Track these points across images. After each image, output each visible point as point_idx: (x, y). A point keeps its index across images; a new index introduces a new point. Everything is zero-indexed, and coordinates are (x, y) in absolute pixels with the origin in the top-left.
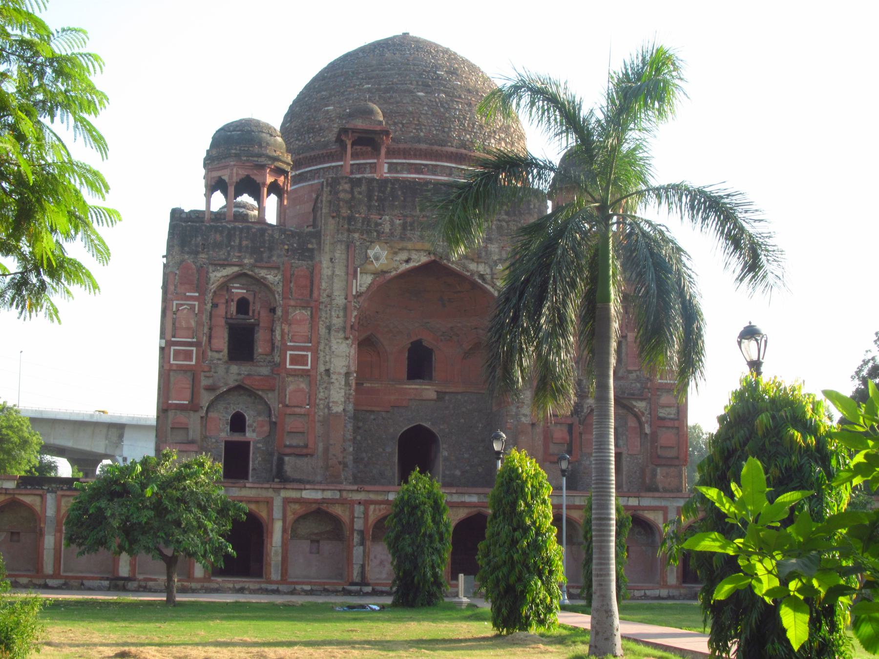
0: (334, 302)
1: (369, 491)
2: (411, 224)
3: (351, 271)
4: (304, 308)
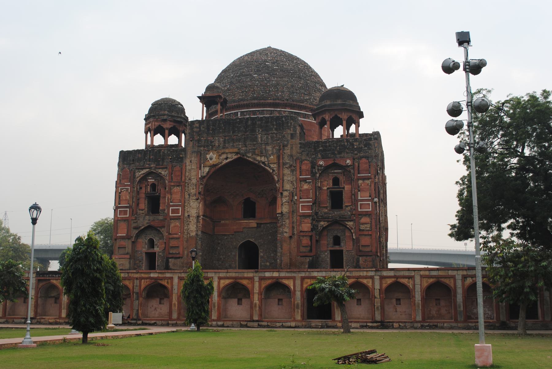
4: (178, 186)
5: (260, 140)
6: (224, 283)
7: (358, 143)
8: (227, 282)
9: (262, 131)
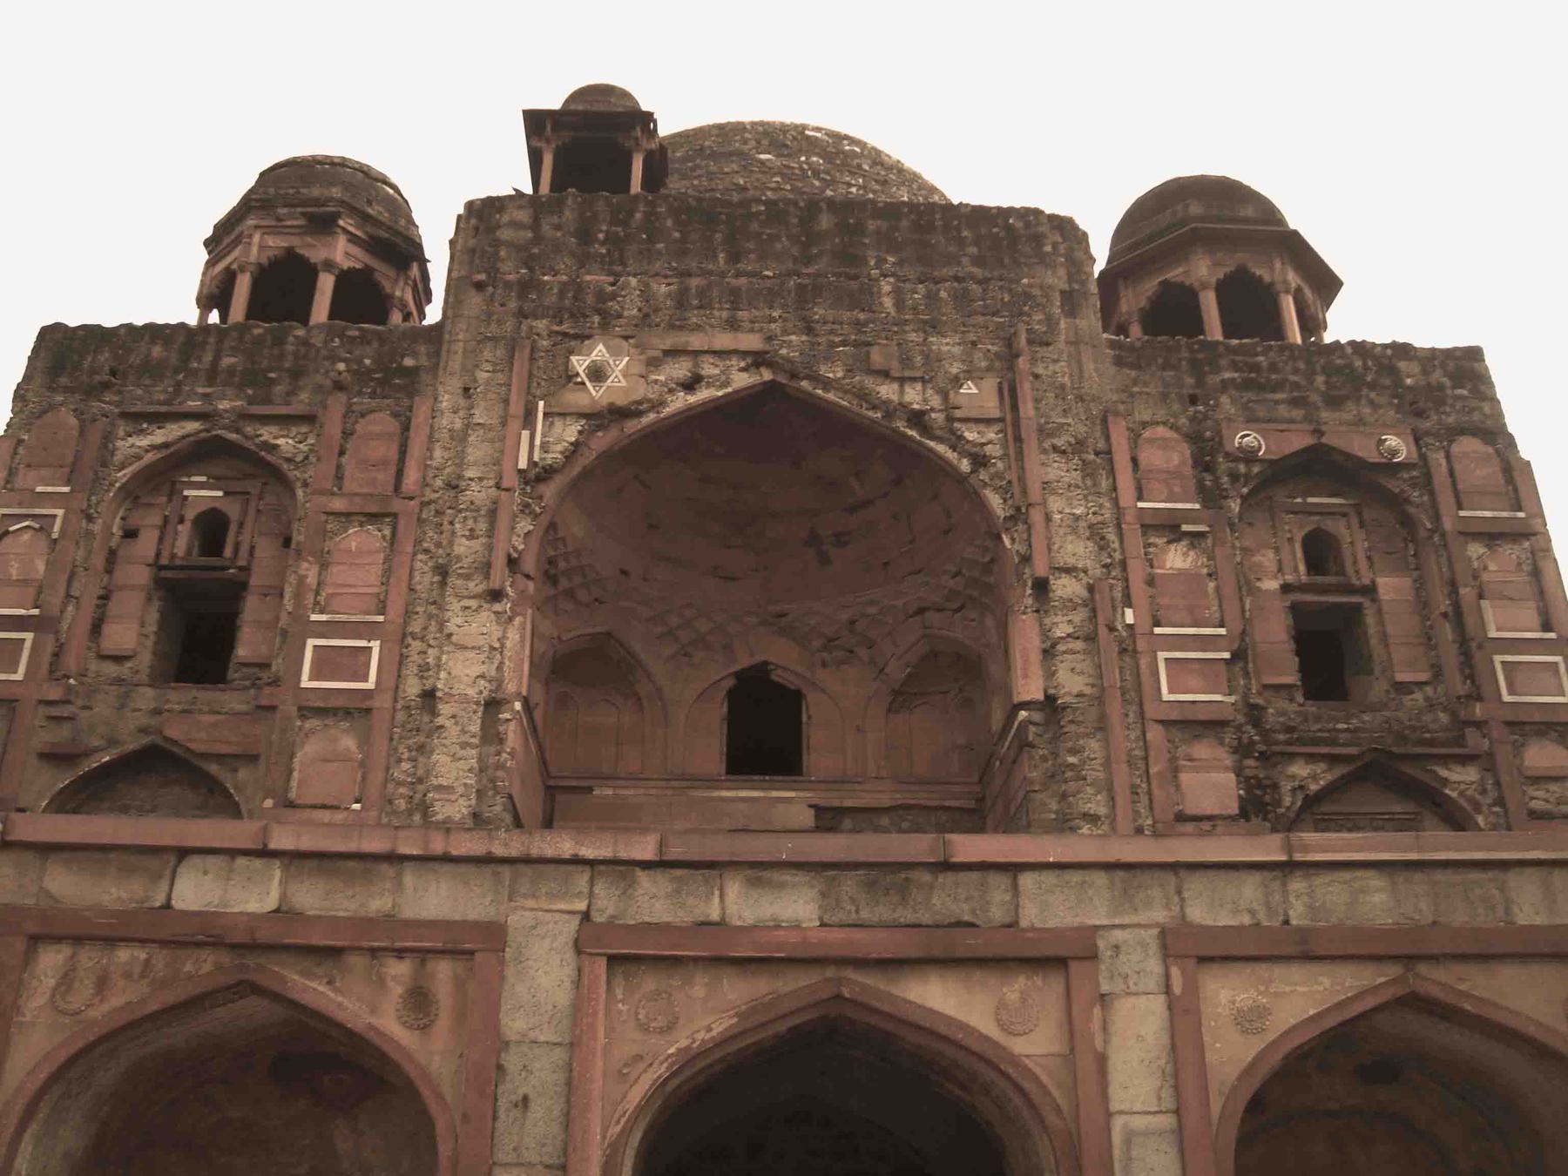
1: (47, 850)
2: (702, 293)
3: (517, 408)
4: (374, 517)
5: (888, 302)
6: (1248, 1020)
7: (1415, 367)
8: (1301, 999)
9: (900, 263)
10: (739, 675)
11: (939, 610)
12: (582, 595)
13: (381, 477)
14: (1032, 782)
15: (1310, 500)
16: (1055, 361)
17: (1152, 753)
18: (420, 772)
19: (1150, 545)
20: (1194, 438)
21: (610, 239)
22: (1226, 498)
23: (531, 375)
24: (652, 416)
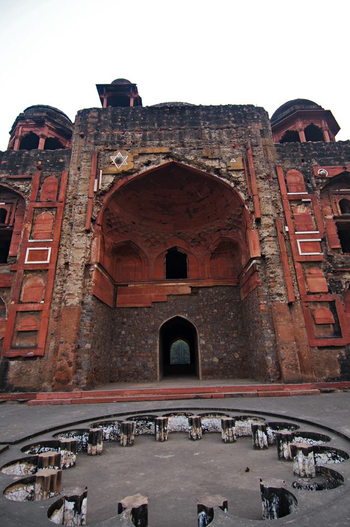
0: (78, 202)
2: (150, 136)
3: (94, 173)
4: (50, 209)
5: (207, 136)
10: (168, 250)
11: (225, 230)
12: (121, 230)
13: (52, 196)
14: (258, 283)
15: (341, 190)
16: (259, 151)
17: (297, 272)
18: (64, 289)
19: (291, 206)
20: (303, 172)
21: (122, 120)
22: (315, 190)
23: (98, 162)
24: (136, 174)
